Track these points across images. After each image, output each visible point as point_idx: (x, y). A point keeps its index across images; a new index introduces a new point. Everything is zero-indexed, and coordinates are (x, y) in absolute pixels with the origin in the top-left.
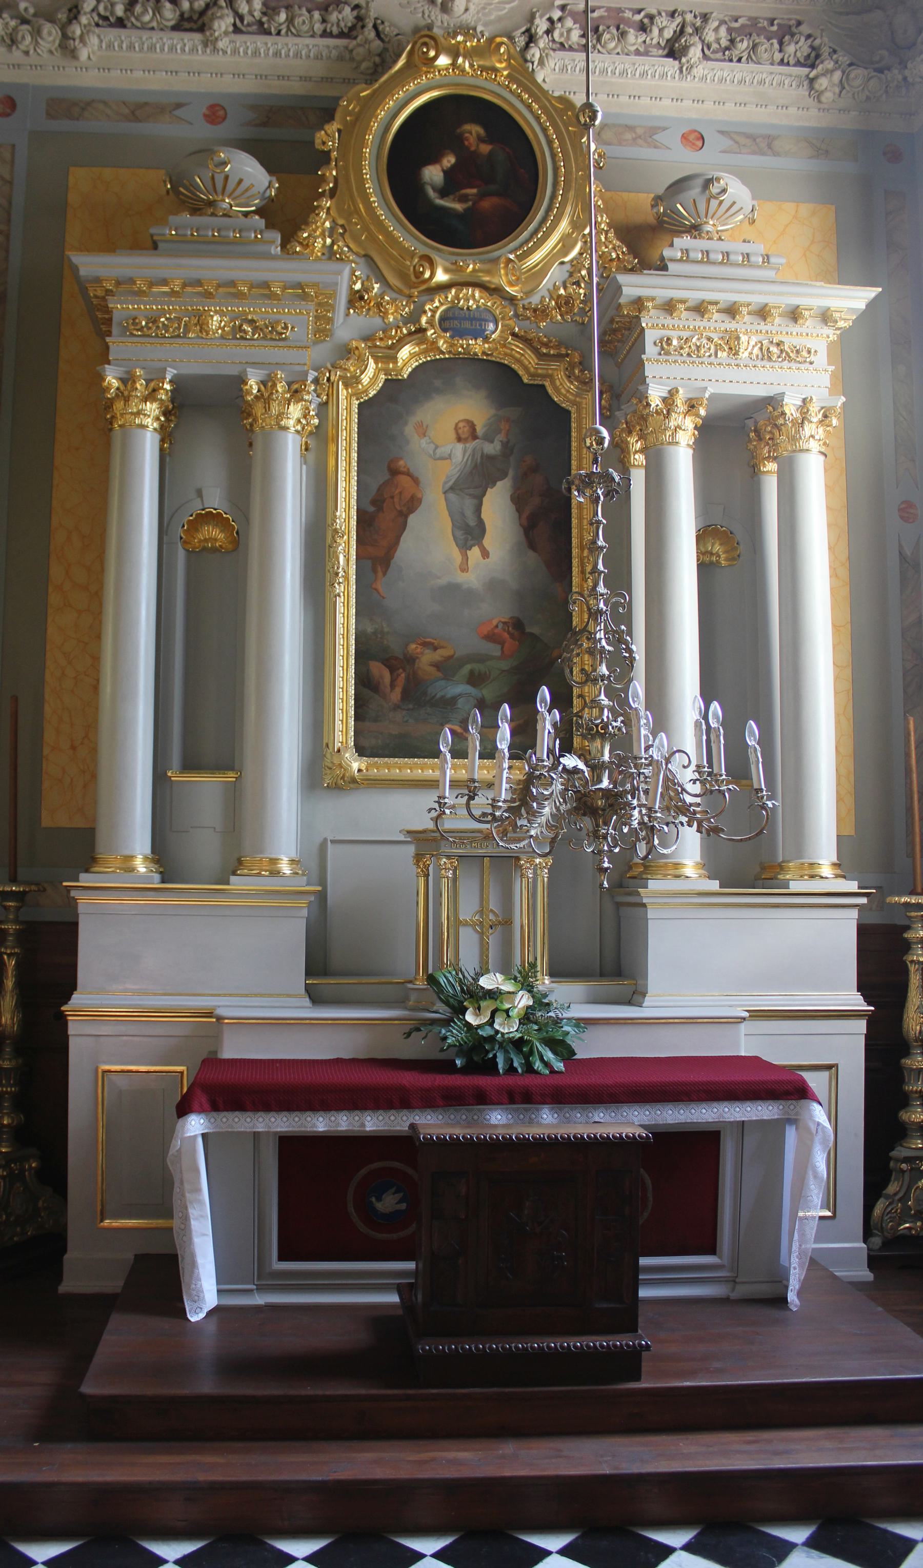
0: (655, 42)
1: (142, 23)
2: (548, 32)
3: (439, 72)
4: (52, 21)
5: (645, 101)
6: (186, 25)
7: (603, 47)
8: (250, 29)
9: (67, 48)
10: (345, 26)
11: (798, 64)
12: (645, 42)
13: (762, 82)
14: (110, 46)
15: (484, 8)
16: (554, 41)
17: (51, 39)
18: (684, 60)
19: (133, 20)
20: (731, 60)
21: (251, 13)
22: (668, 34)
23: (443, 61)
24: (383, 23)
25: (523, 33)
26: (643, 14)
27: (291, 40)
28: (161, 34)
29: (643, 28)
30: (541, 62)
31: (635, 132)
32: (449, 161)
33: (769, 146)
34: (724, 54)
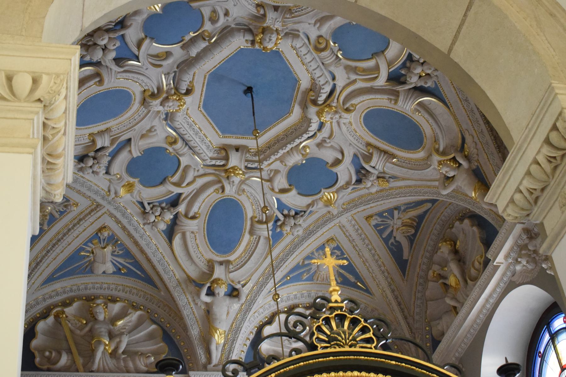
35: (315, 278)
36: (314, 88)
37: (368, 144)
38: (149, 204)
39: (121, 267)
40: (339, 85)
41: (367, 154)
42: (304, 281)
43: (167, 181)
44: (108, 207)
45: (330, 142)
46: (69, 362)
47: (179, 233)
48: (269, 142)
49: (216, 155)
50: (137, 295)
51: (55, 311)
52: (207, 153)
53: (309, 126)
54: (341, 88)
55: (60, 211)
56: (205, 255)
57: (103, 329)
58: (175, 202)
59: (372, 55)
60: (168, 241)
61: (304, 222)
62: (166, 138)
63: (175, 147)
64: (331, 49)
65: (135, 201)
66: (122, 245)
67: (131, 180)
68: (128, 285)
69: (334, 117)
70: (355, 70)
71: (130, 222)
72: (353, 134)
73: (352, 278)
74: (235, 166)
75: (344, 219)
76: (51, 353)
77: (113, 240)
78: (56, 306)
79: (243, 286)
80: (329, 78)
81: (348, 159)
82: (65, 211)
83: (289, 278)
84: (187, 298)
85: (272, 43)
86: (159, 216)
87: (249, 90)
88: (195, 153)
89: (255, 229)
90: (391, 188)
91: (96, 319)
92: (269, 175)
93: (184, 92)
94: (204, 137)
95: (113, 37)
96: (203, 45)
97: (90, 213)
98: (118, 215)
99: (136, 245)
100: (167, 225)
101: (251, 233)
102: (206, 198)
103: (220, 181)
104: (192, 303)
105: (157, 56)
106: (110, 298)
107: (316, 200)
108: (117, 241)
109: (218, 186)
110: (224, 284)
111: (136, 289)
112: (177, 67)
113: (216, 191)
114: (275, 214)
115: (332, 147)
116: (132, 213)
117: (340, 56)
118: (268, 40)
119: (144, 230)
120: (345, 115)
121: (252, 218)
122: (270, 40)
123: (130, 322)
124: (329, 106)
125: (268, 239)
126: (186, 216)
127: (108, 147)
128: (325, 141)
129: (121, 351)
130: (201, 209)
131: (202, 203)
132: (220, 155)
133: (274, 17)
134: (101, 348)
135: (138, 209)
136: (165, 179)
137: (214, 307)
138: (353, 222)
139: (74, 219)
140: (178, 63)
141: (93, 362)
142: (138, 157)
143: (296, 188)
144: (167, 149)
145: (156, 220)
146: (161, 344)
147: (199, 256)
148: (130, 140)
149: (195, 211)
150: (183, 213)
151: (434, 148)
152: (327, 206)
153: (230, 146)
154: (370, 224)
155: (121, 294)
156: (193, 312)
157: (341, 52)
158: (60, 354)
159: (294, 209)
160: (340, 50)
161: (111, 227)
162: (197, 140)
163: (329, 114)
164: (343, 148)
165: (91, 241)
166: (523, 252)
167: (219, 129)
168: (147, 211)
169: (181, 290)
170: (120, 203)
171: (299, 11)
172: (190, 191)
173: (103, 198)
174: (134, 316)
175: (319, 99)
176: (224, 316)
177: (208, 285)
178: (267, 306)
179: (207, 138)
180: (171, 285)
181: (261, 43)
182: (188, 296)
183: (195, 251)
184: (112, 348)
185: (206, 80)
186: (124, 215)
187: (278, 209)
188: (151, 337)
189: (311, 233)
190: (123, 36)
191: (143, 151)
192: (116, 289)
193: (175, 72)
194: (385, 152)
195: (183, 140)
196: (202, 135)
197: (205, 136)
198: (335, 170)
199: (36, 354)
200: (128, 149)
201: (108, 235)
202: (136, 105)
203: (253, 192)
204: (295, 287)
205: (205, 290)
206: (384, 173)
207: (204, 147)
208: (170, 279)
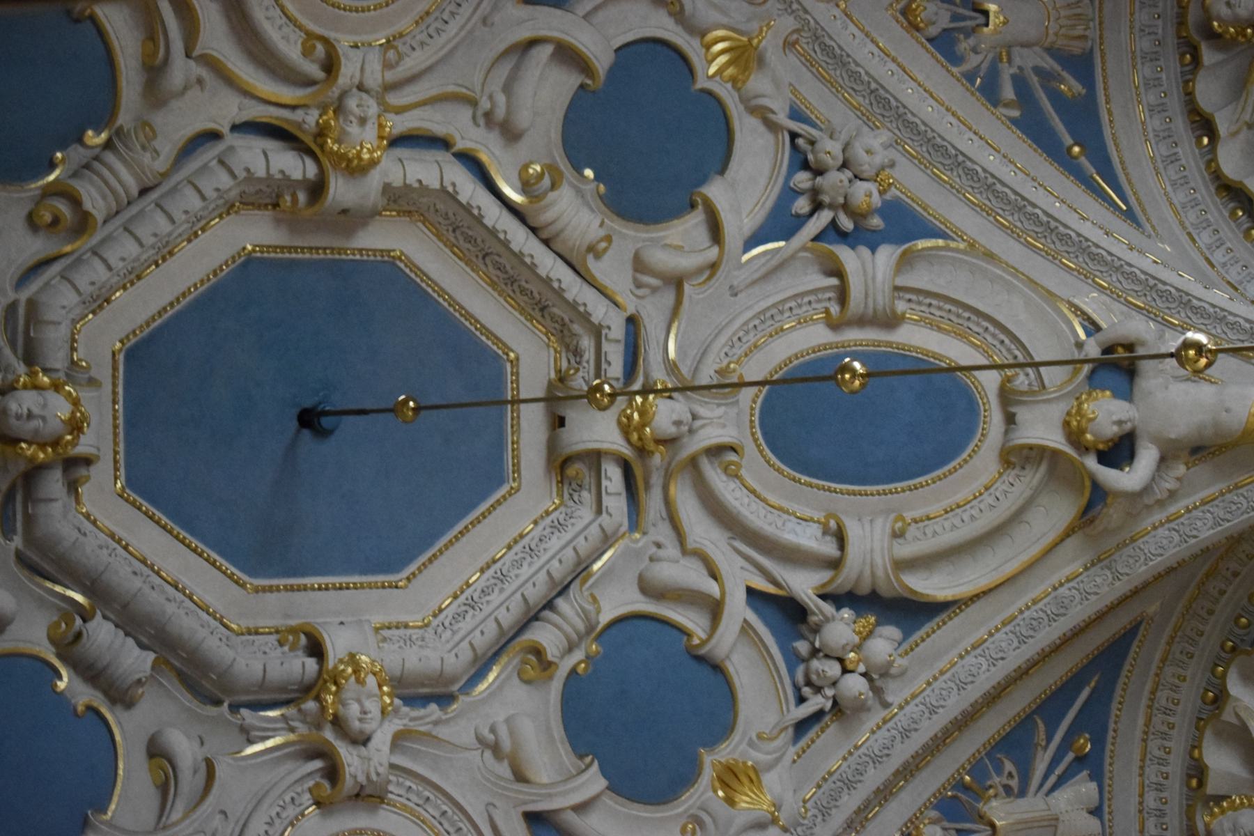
35: (1076, 48)
38: (801, 700)
39: (1070, 756)
40: (236, 110)
43: (702, 652)
45: (491, 97)
48: (522, 311)
49: (585, 494)
50: (1175, 688)
52: (580, 525)
53: (423, 188)
54: (247, 102)
56: (984, 480)
59: (77, 21)
60: (944, 616)
62: (528, 682)
63: (552, 652)
64: (75, 175)
65: (792, 751)
66: (976, 768)
67: (708, 774)
68: (1141, 721)
69: (357, 111)
70: (154, 71)
71: (876, 760)
72: (439, 24)
74: (619, 423)
79: (1093, 327)
80: (209, 154)
83: (1076, 149)
84: (1155, 528)
85: (45, 406)
86: (841, 660)
87: (309, 419)
88: (581, 570)
89: (870, 311)
92: (654, 290)
93: (311, 664)
94: (517, 548)
98: (850, 803)
99: (918, 768)
100: (878, 623)
101: (891, 321)
102: (764, 501)
104: (1172, 509)
105: (165, 789)
106: (1194, 782)
107: (745, 100)
108: (966, 788)
110: (1080, 405)
111: (1153, 693)
112: (218, 703)
113: (733, 474)
114: (810, 244)
115: (507, 88)
116: (844, 752)
117: (104, 136)
119: (907, 703)
120: (348, 71)
122: (30, 415)
124: (321, 133)
125: (905, 262)
126: (835, 565)
128: (488, 115)
130: (808, 513)
131: (787, 512)
132: (587, 480)
136: (701, 659)
137: (1173, 436)
142: (604, 772)
143: (704, 180)
144: (573, 671)
145: (862, 668)
147: (988, 499)
149: (819, 534)
150: (822, 576)
152: (761, 61)
153: (552, 446)
155: (1178, 744)
156: (1204, 503)
157: (90, 133)
160: (80, 140)
161: (907, 814)
162: (526, 571)
163: (344, 132)
164: (503, 47)
167: (484, 497)
168: (829, 704)
169: (1129, 550)
170: (805, 802)
172: (741, 562)
175: (297, 175)
177: (1091, 462)
178: (1191, 216)
179: (522, 536)
181: (56, 443)
182: (1147, 523)
183: (954, 527)
185: (275, 582)
186: (849, 785)
187: (787, 235)
191: (581, 757)
192: (1162, 762)
193: (234, 708)
195: (523, 627)
196: (511, 556)
197: (516, 542)
200: (571, 818)
201: (934, 822)
203: (723, 339)
204: (1116, 113)
205: (1111, 477)
207: (555, 543)
208: (961, 686)
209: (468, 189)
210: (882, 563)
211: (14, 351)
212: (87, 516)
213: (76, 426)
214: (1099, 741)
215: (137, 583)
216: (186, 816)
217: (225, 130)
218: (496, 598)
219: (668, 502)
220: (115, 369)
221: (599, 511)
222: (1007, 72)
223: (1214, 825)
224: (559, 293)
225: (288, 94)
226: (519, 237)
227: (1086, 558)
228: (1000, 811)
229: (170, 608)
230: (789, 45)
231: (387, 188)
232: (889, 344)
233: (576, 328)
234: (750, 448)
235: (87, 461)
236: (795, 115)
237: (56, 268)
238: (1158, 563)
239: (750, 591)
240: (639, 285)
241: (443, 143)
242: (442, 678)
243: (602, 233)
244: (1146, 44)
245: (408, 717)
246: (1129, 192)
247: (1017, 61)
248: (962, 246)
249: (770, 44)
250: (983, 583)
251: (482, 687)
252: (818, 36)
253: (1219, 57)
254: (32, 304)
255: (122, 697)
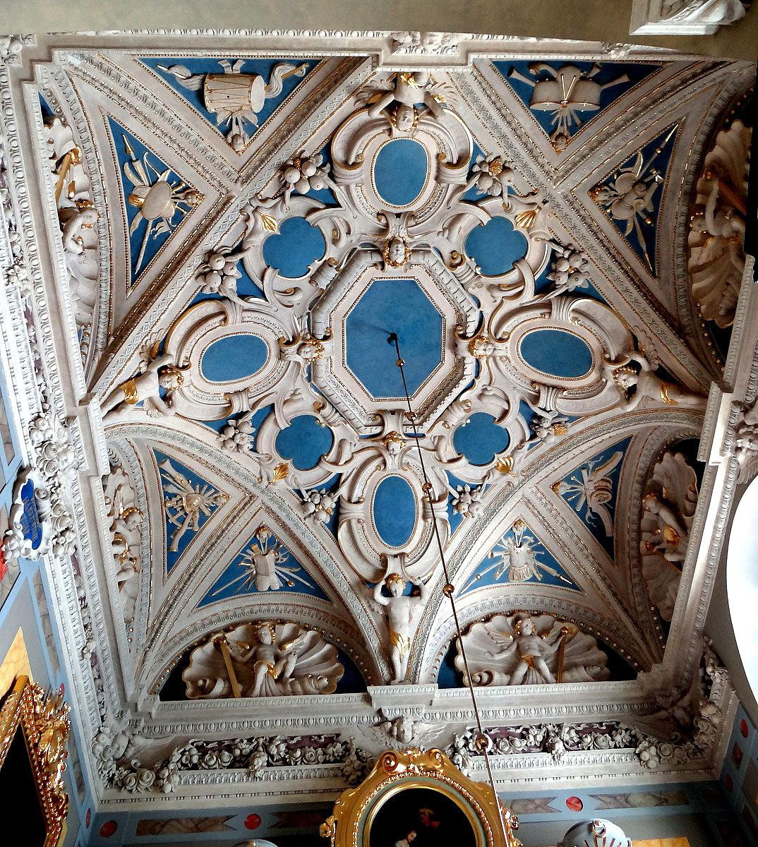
0: (533, 744)
1: (209, 766)
2: (466, 746)
3: (399, 775)
4: (151, 769)
5: (536, 782)
6: (237, 765)
7: (501, 751)
8: (277, 763)
9: (158, 787)
10: (338, 755)
11: (626, 746)
12: (526, 745)
13: (607, 760)
14: (186, 782)
15: (424, 736)
16: (470, 751)
17: (149, 779)
18: (553, 752)
19: (203, 764)
20: (583, 749)
21: (278, 753)
22: (540, 738)
23: (401, 768)
24: (361, 751)
25: (450, 748)
26: (521, 728)
27: (304, 767)
28: (220, 771)
29: (523, 737)
30: (464, 764)
31: (535, 803)
32: (412, 836)
33: (627, 801)
34: (578, 747)
36: (462, 322)
37: (533, 382)
38: (307, 491)
39: (288, 580)
41: (534, 393)
42: (498, 582)
44: (263, 498)
46: (226, 689)
47: (344, 522)
51: (215, 637)
53: (464, 370)
54: (489, 316)
55: (211, 507)
57: (267, 652)
58: (334, 486)
61: (484, 501)
66: (284, 549)
67: (285, 462)
70: (499, 287)
72: (513, 374)
73: (554, 573)
75: (528, 489)
76: (205, 681)
77: (273, 543)
78: (216, 633)
80: (474, 304)
81: (515, 407)
82: (217, 506)
86: (319, 504)
87: (393, 338)
90: (571, 437)
91: (262, 643)
92: (433, 443)
93: (321, 337)
95: (230, 261)
96: (331, 273)
97: (243, 508)
98: (275, 508)
101: (425, 517)
103: (381, 455)
108: (278, 545)
109: (378, 461)
112: (310, 309)
113: (378, 467)
117: (479, 273)
118: (395, 252)
120: (499, 345)
121: (423, 499)
123: (301, 644)
124: (481, 338)
125: (444, 521)
126: (349, 501)
127: (247, 412)
129: (288, 674)
133: (398, 224)
134: (263, 670)
135: (295, 500)
136: (320, 459)
138: (539, 495)
139: (228, 517)
140: (309, 302)
141: (254, 688)
143: (467, 458)
145: (317, 510)
146: (337, 665)
147: (370, 550)
148: (272, 407)
150: (345, 496)
151: (605, 359)
153: (385, 411)
154: (557, 494)
155: (291, 616)
158: (215, 682)
159: (469, 485)
162: (347, 403)
165: (249, 547)
166: (742, 431)
169: (355, 596)
171: (423, 216)
173: (255, 485)
174: (307, 637)
176: (406, 619)
177: (383, 583)
180: (343, 589)
181: (389, 258)
182: (363, 602)
184: (279, 672)
188: (325, 658)
189: (493, 512)
190: (242, 260)
193: (308, 314)
194: (554, 387)
198: (503, 424)
199: (189, 684)
200: (271, 419)
202: (272, 360)
204: (490, 591)
206: (560, 415)
207: (356, 412)
209: (464, 384)
210: (350, 516)
211: (417, 247)
212: (366, 269)
213: (395, 264)
214: (292, 589)
215: (347, 284)
216: (278, 299)
217: (481, 309)
218: (340, 394)
219: (368, 448)
220: (409, 277)
221: (365, 426)
222: (502, 554)
223: (266, 628)
224: (432, 412)
225: (493, 328)
226: (449, 400)
227: (351, 582)
228: (271, 557)
229: (339, 294)
230: (509, 483)
231: (464, 358)
232: (418, 517)
233: (422, 418)
234: (386, 473)
235: (383, 269)
236: (488, 486)
237: (440, 259)
238: (351, 606)
239: (341, 475)
240: (434, 438)
241: (477, 376)
242: (315, 377)
243: (451, 425)
244: (512, 600)
245: (304, 366)
246: (467, 594)
247: (506, 557)
248: (449, 540)
249: (509, 477)
250: (344, 549)
251: (312, 390)
252: (512, 493)
253: (510, 623)
254: (430, 251)
255: (312, 280)
